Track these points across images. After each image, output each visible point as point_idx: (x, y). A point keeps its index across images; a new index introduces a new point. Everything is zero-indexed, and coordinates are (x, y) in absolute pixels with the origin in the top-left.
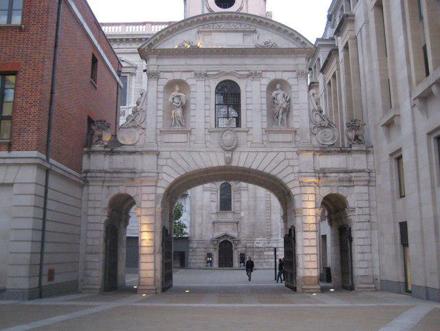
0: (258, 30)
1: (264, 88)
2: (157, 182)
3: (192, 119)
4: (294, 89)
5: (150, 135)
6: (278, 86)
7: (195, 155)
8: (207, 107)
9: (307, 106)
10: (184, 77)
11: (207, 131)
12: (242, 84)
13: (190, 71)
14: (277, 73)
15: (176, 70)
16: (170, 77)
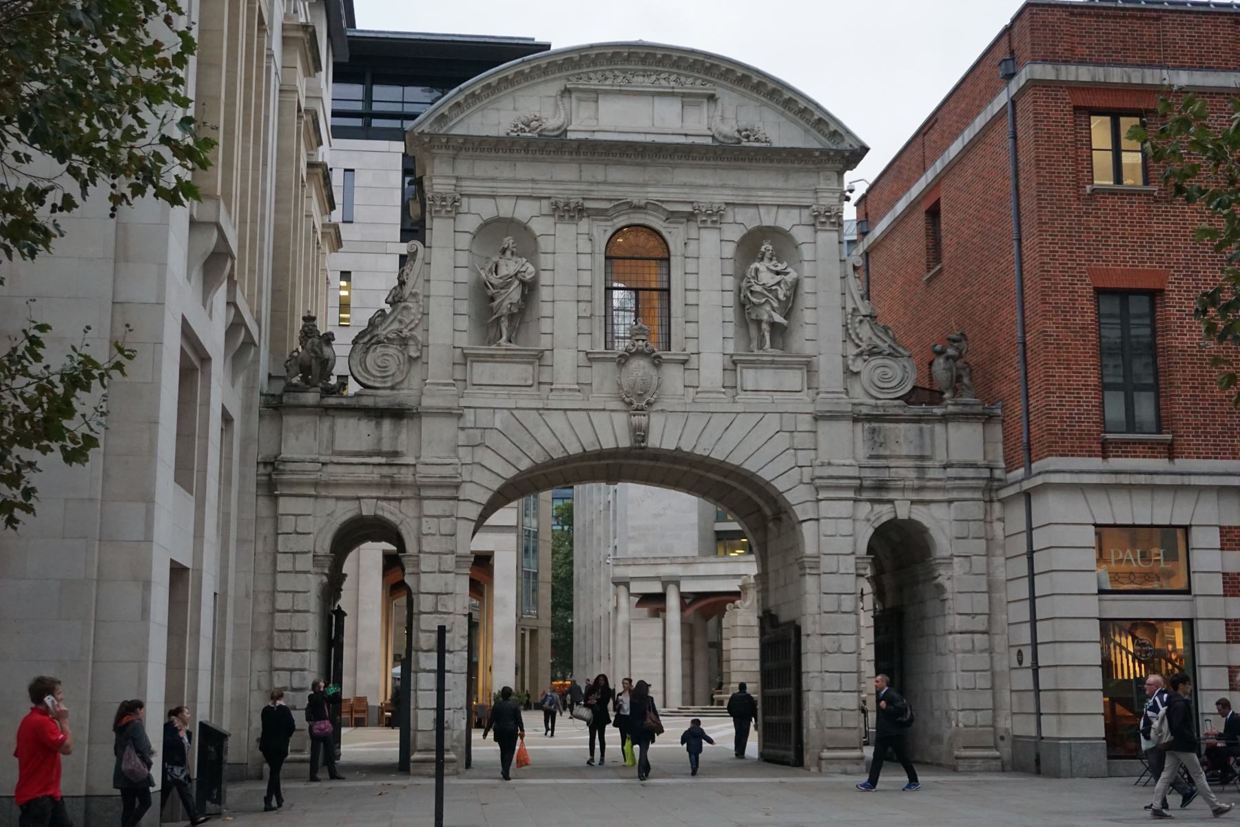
0: (719, 92)
1: (729, 250)
2: (457, 487)
3: (545, 326)
4: (807, 252)
5: (438, 366)
6: (766, 247)
7: (556, 420)
8: (585, 294)
9: (837, 298)
10: (524, 211)
11: (582, 355)
12: (675, 236)
13: (540, 198)
14: (762, 210)
15: (507, 192)
16: (487, 209)
